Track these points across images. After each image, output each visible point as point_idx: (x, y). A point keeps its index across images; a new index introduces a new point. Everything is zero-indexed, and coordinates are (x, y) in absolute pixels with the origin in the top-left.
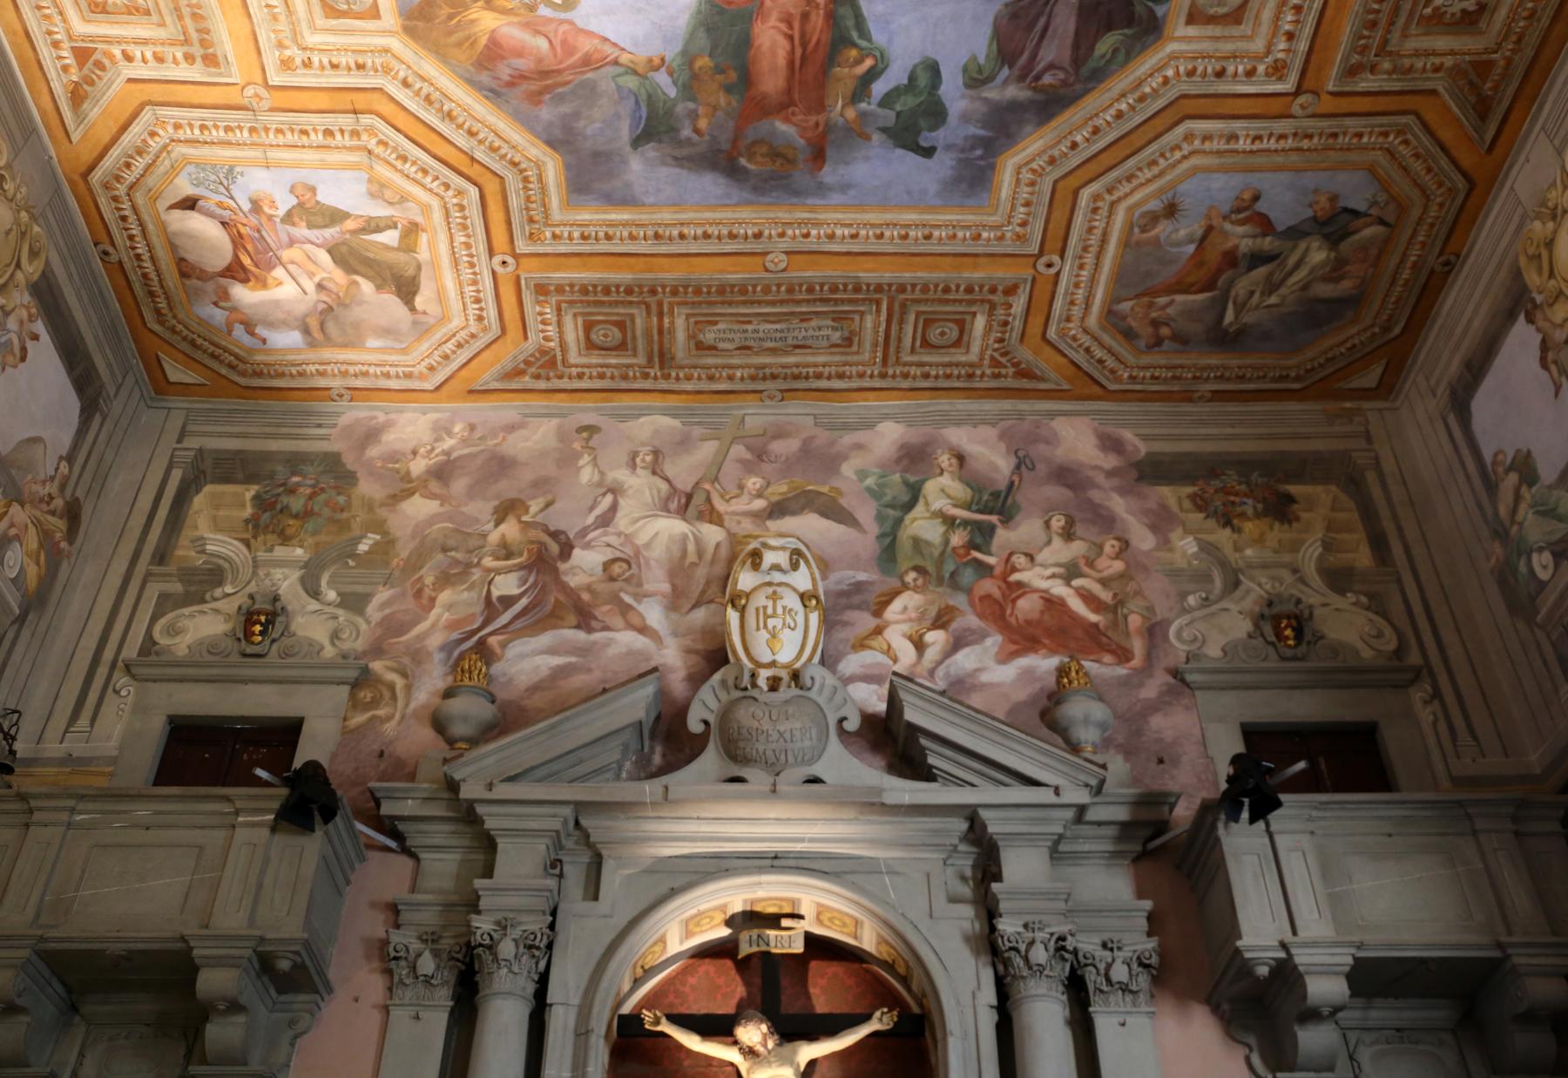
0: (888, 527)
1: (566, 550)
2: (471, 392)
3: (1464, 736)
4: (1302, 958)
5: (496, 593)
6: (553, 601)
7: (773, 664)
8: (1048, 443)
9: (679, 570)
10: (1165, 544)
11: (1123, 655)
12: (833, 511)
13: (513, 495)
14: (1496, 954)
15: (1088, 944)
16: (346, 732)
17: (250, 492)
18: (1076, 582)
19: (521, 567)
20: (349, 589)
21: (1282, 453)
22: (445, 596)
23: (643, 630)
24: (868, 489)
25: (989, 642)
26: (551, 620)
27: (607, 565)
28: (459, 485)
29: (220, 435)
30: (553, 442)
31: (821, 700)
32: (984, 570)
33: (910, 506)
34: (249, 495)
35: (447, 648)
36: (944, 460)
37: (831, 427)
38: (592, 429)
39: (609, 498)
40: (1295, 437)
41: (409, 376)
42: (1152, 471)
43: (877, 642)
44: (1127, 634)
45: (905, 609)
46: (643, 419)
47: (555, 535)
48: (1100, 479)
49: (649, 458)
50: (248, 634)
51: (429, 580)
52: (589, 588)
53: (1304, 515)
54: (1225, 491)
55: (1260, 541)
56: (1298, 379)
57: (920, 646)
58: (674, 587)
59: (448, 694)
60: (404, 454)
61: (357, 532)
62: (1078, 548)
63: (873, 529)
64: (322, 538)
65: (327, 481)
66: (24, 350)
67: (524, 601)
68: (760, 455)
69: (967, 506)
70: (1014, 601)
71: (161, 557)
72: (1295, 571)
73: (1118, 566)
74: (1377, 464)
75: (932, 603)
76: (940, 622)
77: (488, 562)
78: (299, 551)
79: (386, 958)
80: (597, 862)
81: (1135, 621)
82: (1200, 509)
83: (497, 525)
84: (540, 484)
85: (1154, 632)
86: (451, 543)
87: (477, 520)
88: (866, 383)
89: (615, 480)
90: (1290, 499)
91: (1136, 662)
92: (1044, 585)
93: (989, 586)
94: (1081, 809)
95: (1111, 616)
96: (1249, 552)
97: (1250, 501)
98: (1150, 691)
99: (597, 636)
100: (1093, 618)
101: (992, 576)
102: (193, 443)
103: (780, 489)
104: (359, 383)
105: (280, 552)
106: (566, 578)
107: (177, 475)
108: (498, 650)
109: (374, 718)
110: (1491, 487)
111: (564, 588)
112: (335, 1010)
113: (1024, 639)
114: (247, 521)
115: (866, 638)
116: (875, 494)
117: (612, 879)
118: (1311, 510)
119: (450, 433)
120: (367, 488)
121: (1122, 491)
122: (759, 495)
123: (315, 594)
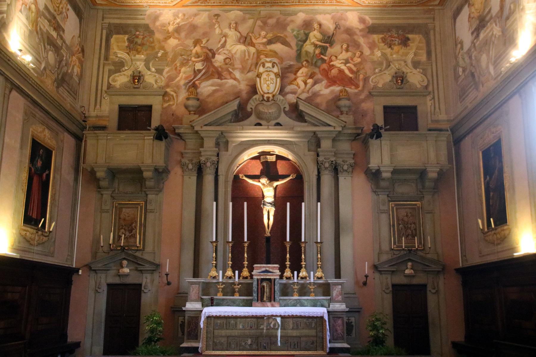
0: (299, 48)
1: (213, 56)
2: (183, 6)
3: (437, 110)
4: (382, 169)
5: (196, 68)
6: (213, 72)
7: (268, 93)
8: (345, 20)
9: (243, 61)
10: (372, 53)
11: (357, 86)
12: (285, 43)
13: (198, 38)
14: (424, 168)
15: (340, 161)
16: (163, 108)
17: (126, 37)
18: (348, 65)
19: (202, 61)
20: (158, 67)
21: (409, 24)
22: (183, 69)
23: (235, 79)
24: (294, 35)
25: (323, 82)
26: (211, 76)
27: (225, 60)
28: (183, 34)
29: (114, 18)
30: (207, 20)
31: (279, 103)
32: (324, 61)
33: (305, 41)
34: (126, 38)
35: (185, 84)
39: (224, 39)
40: (413, 18)
41: (166, 3)
43: (295, 83)
44: (359, 81)
45: (303, 72)
46: (232, 12)
47: (210, 50)
48: (358, 32)
49: (234, 25)
50: (134, 82)
51: (178, 65)
52: (220, 67)
53: (411, 44)
54: (391, 36)
56: (416, 3)
57: (306, 83)
58: (243, 66)
59: (188, 99)
60: (166, 24)
61: (157, 50)
62: (349, 54)
63: (295, 48)
64: (148, 52)
65: (146, 34)
66: (67, 15)
67: (204, 71)
69: (321, 41)
70: (331, 70)
71: (106, 58)
72: (405, 62)
73: (359, 60)
75: (308, 71)
76: (311, 77)
77: (193, 59)
78: (143, 56)
79: (183, 166)
81: (361, 77)
82: (384, 42)
83: (194, 48)
84: (205, 34)
85: (366, 80)
86: (183, 53)
87: (189, 46)
88: (294, 4)
89: (225, 33)
90: (408, 39)
91: (360, 89)
92: (339, 65)
93: (325, 66)
94: (340, 132)
95: (355, 75)
96: (394, 56)
97: (397, 40)
98: (362, 97)
99: (223, 81)
100: (351, 75)
101: (325, 63)
102: (107, 21)
103: (270, 35)
104: (152, 4)
105: (138, 56)
106: (214, 64)
107: (105, 32)
108: (198, 85)
109: (169, 105)
110: (456, 45)
111: (214, 67)
112: (172, 176)
113: (332, 82)
114: (127, 47)
115: (292, 81)
116: (296, 37)
118: (413, 43)
119: (178, 17)
120: (158, 36)
121: (363, 36)
122: (265, 38)
123: (149, 69)
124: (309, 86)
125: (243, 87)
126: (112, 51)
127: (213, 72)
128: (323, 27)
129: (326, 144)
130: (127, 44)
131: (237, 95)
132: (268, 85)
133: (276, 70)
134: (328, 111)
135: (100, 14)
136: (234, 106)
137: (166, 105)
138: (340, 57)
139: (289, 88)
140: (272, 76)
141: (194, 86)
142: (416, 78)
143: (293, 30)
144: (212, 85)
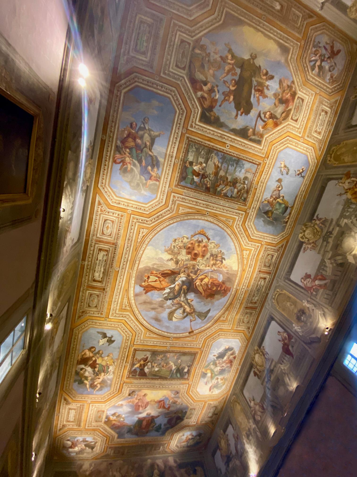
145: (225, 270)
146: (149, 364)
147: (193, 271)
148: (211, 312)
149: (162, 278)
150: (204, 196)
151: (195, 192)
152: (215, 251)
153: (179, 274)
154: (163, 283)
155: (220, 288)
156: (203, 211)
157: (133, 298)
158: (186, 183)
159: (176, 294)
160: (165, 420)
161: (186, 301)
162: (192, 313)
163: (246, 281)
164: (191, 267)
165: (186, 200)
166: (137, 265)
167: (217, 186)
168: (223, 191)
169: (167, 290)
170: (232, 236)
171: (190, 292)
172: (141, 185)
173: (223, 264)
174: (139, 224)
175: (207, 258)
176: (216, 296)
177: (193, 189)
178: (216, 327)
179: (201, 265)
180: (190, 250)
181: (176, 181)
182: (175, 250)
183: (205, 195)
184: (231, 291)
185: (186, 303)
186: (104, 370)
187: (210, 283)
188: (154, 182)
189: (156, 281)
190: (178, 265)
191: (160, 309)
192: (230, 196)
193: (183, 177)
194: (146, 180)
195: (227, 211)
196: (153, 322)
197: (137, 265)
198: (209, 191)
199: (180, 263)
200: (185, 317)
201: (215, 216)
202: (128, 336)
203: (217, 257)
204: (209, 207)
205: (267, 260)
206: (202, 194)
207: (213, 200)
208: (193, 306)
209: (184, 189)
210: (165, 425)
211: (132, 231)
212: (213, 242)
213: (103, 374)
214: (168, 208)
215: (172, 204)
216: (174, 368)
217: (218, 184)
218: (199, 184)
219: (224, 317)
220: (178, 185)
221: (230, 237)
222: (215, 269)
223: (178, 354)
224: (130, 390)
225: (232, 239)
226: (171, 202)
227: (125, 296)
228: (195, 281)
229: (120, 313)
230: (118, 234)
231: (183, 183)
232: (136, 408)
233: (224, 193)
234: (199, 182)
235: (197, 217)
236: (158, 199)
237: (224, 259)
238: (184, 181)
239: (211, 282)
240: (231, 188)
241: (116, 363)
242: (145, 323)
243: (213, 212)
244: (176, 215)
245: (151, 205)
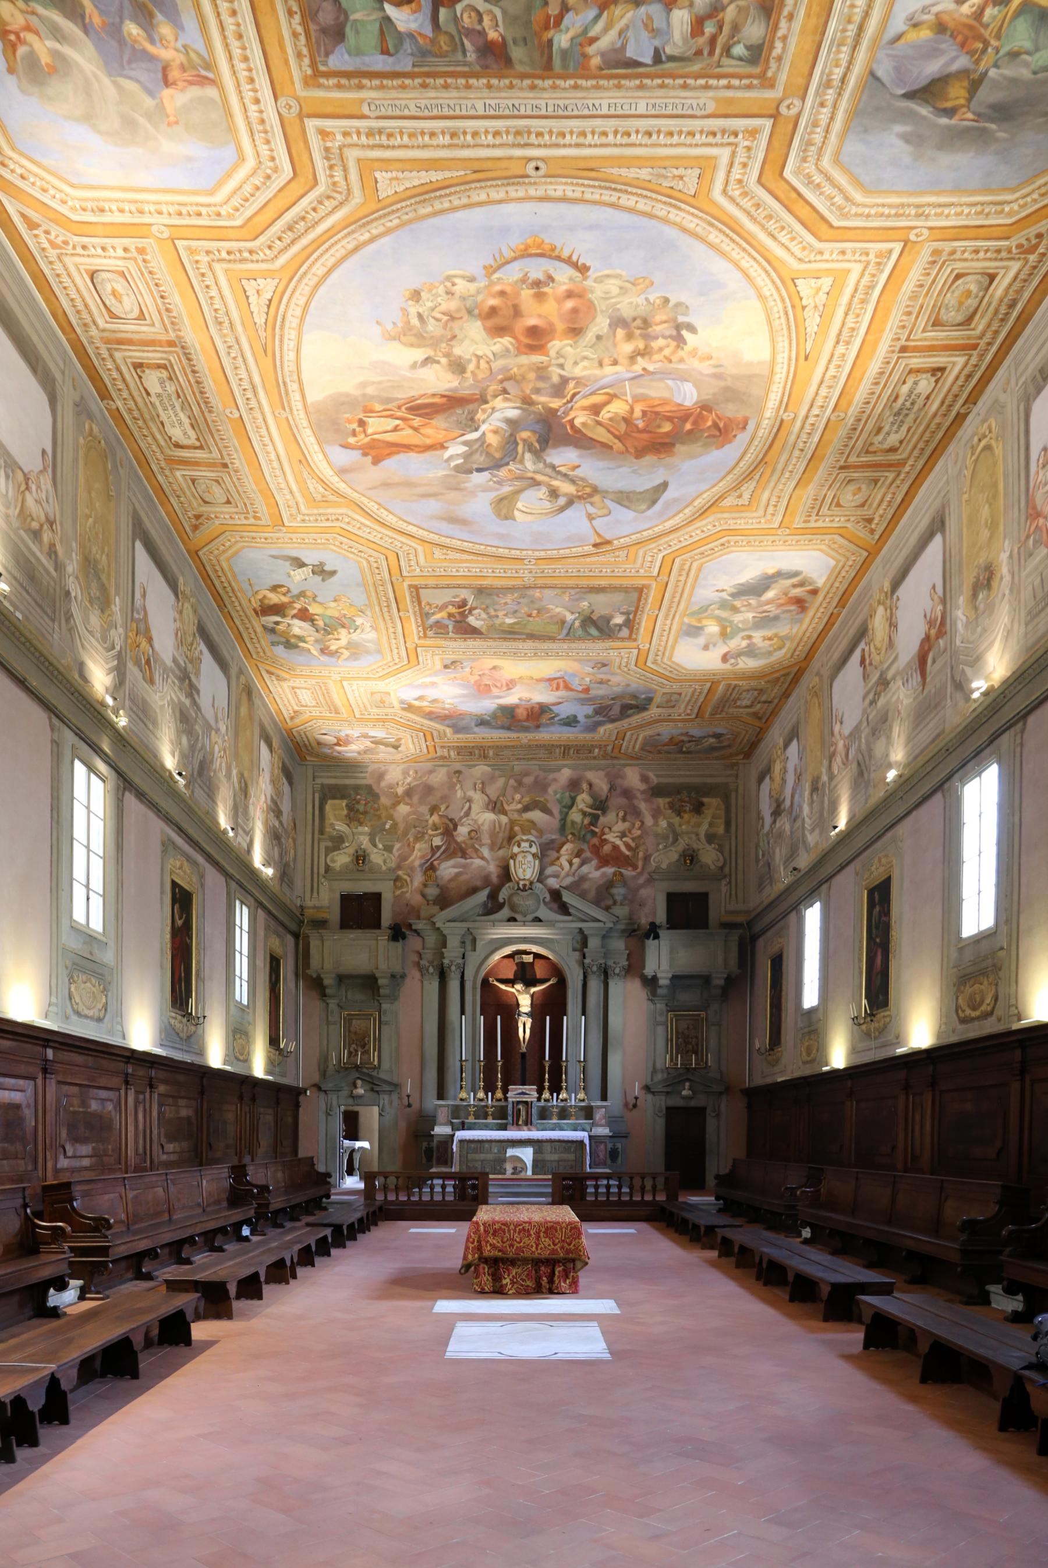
9: (493, 835)
12: (546, 810)
17: (344, 803)
23: (483, 858)
27: (469, 833)
30: (445, 779)
33: (571, 807)
36: (585, 786)
37: (545, 771)
38: (459, 772)
40: (711, 776)
42: (657, 791)
48: (639, 795)
54: (681, 800)
55: (688, 822)
62: (627, 825)
68: (520, 783)
74: (737, 791)
80: (474, 940)
82: (671, 808)
102: (319, 781)
103: (527, 799)
111: (456, 842)
116: (560, 801)
117: (479, 945)
121: (645, 800)
124: (574, 867)
125: (493, 869)
126: (327, 822)
127: (456, 850)
128: (595, 788)
129: (594, 943)
130: (345, 812)
131: (487, 881)
132: (525, 869)
133: (534, 850)
134: (597, 902)
135: (310, 772)
136: (483, 896)
137: (398, 892)
138: (615, 829)
139: (549, 871)
140: (530, 858)
141: (432, 868)
142: (709, 856)
143: (556, 793)
144: (454, 867)
145: (705, 368)
146: (475, 612)
147: (540, 385)
148: (670, 488)
149: (417, 421)
150: (486, 93)
151: (424, 86)
152: (630, 304)
153: (486, 402)
154: (428, 431)
155: (695, 423)
156: (504, 164)
157: (336, 479)
158: (358, 52)
159: (497, 455)
160: (589, 710)
161: (549, 471)
162: (590, 495)
163: (823, 392)
164: (532, 376)
165: (390, 135)
166: (296, 396)
167: (547, 27)
168: (593, 40)
169: (456, 449)
170: (714, 237)
171: (555, 446)
172: (141, 120)
173: (688, 348)
174: (225, 265)
175: (599, 338)
176: (679, 448)
177: (411, 75)
178: (708, 525)
179: (576, 363)
180: (499, 319)
181: (299, 55)
182: (430, 328)
183: (489, 87)
184: (751, 427)
185: (553, 474)
186: (342, 623)
187: (638, 413)
188: (195, 91)
189: (396, 429)
190: (468, 374)
191: (452, 495)
192: (648, 60)
193: (324, 31)
194: (151, 93)
195: (649, 134)
196: (444, 527)
197: (296, 396)
198: (508, 62)
199: (471, 367)
200: (562, 509)
201: (586, 171)
202: (372, 559)
203: (646, 323)
204: (533, 139)
205: (951, 299)
206: (468, 87)
207: (548, 97)
208: (582, 479)
209: (361, 87)
210: (587, 717)
211: (213, 292)
212: (608, 276)
213: (343, 632)
214: (321, 189)
215: (331, 167)
216: (569, 617)
217: (553, 10)
218: (433, 41)
219: (740, 496)
220: (317, 74)
221: (703, 240)
222: (651, 368)
223: (573, 592)
224: (442, 660)
225: (711, 246)
226: (320, 164)
227: (305, 474)
228: (566, 413)
229: (316, 511)
230: (168, 310)
231: (340, 59)
232: (483, 689)
233: (603, 54)
234: (428, 31)
235: (483, 197)
236: (251, 162)
237: (691, 328)
238: (340, 49)
239: (644, 413)
240: (643, 9)
241: (369, 613)
242: (412, 529)
243: (563, 158)
244: (374, 206)
245: (234, 192)
